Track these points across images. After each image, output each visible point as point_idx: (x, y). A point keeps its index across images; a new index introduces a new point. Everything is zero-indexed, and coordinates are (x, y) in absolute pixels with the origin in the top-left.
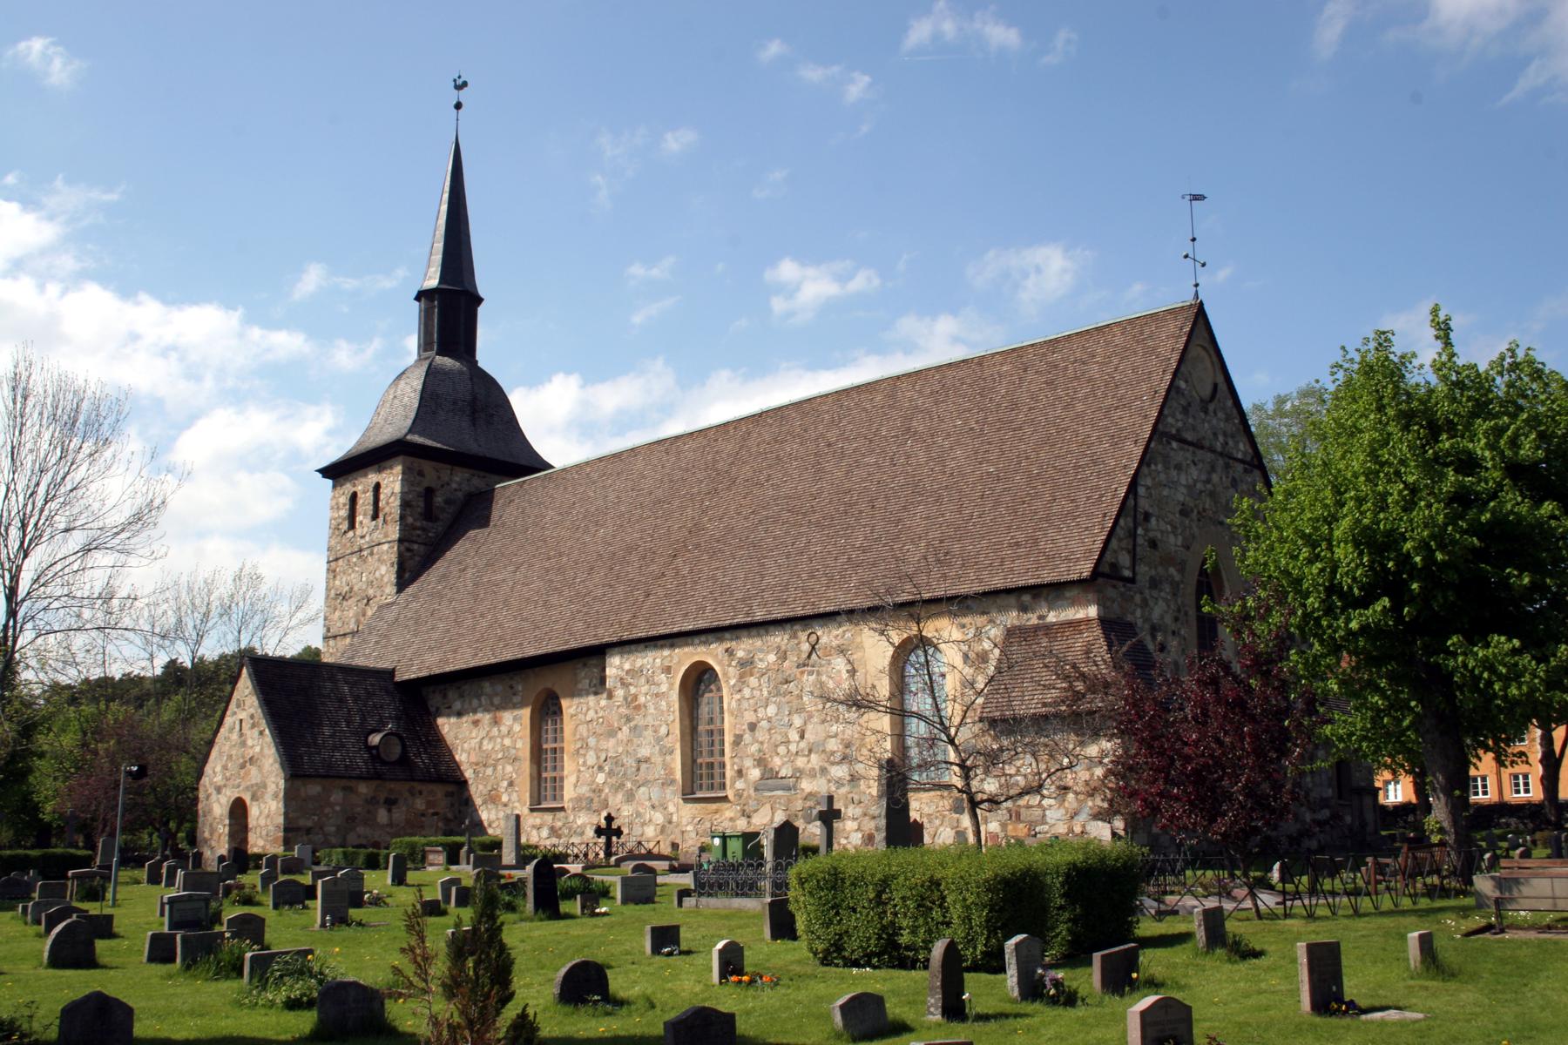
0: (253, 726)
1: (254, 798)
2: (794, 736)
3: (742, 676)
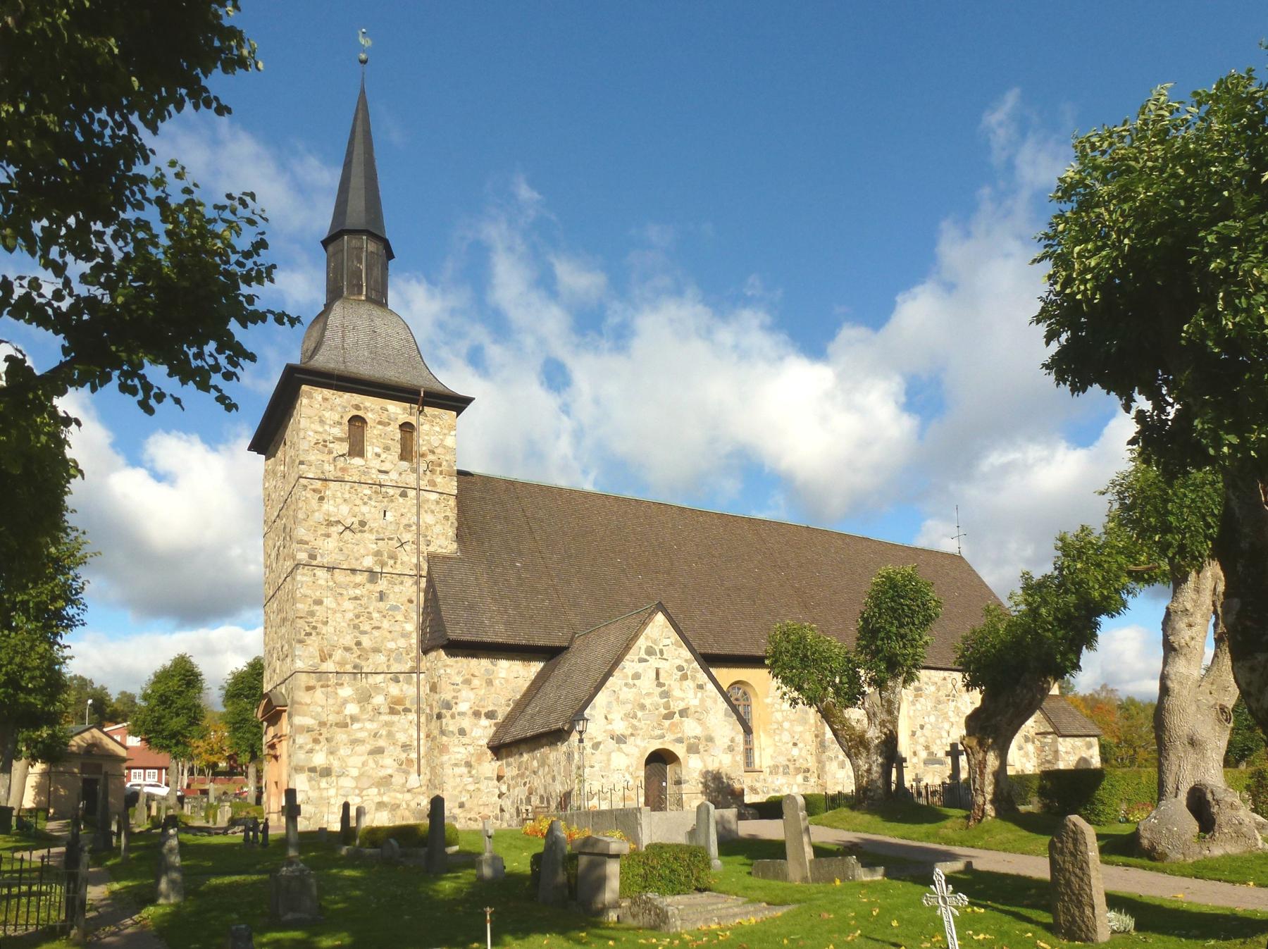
0: (684, 677)
1: (693, 749)
2: (945, 734)
3: (916, 696)
